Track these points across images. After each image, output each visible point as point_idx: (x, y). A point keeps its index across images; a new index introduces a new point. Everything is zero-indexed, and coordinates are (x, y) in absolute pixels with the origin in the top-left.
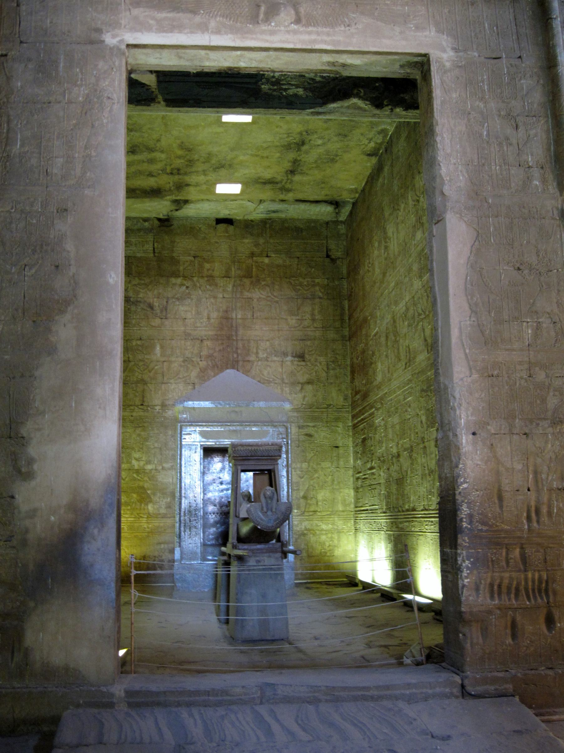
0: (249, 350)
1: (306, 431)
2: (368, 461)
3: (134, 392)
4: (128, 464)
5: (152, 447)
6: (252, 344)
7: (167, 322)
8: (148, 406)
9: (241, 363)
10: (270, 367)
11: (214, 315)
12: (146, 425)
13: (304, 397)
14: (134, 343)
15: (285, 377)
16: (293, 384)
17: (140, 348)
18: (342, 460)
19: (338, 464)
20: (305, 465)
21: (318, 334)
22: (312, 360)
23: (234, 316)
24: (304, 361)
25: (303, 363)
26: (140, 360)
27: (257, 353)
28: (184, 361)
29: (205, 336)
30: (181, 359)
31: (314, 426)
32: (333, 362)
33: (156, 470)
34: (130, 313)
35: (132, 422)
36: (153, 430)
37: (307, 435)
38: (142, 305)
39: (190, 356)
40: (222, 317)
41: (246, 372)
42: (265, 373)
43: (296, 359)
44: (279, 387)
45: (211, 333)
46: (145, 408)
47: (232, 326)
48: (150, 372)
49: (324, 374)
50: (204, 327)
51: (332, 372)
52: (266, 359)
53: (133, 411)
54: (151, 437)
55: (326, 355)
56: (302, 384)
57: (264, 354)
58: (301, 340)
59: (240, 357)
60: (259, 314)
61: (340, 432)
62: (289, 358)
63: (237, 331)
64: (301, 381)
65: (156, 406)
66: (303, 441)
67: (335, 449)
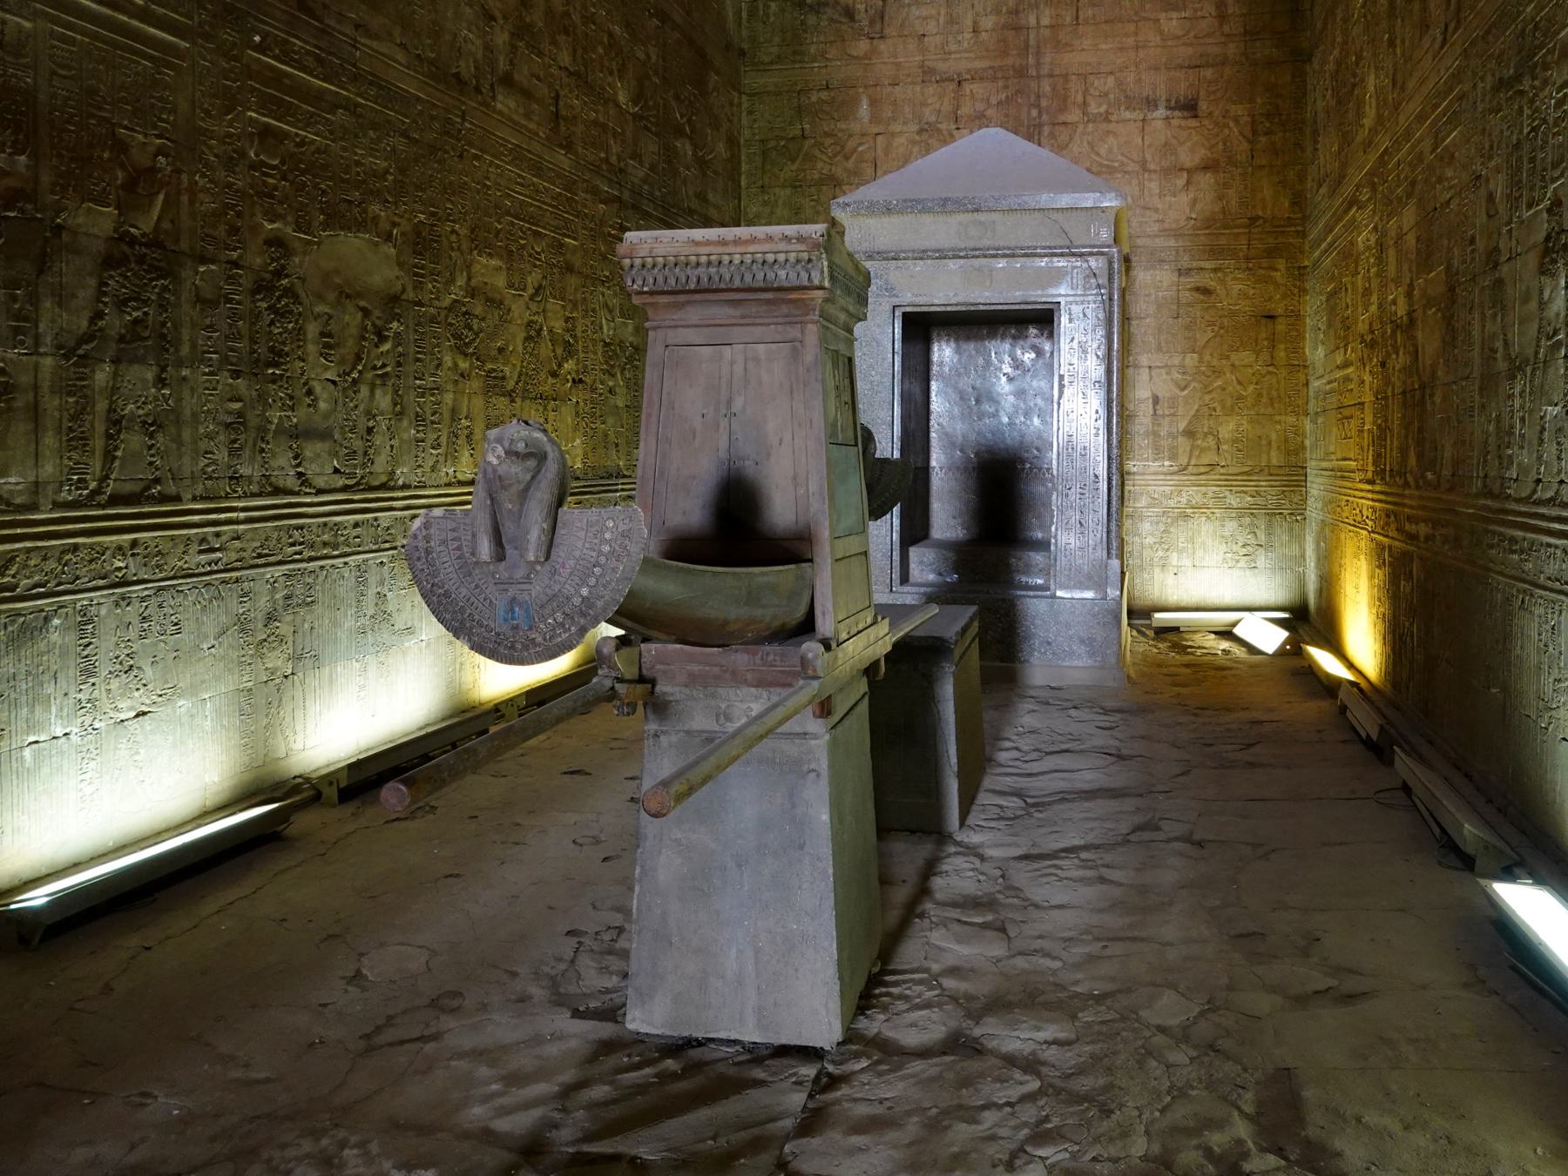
0: (1065, 98)
1: (1195, 280)
6: (1075, 86)
7: (883, 46)
9: (1046, 130)
10: (1115, 134)
11: (988, 22)
13: (1195, 201)
14: (814, 99)
15: (1148, 157)
16: (1166, 172)
17: (826, 108)
18: (1282, 346)
20: (1191, 360)
21: (1232, 50)
22: (1216, 113)
23: (1032, 20)
24: (1196, 117)
25: (1193, 123)
26: (826, 134)
27: (1085, 103)
28: (920, 132)
29: (969, 71)
30: (916, 128)
31: (1215, 270)
32: (1268, 116)
34: (805, 31)
37: (1197, 289)
38: (829, 10)
39: (933, 119)
40: (1005, 27)
41: (1060, 149)
42: (1103, 151)
43: (1177, 113)
44: (1135, 182)
45: (979, 64)
47: (1027, 46)
48: (847, 158)
49: (1245, 146)
50: (967, 51)
51: (1263, 139)
52: (1106, 118)
55: (1252, 100)
56: (1189, 171)
57: (1100, 105)
58: (1190, 67)
59: (1045, 117)
60: (1090, 12)
61: (1279, 280)
62: (1161, 112)
63: (1038, 53)
64: (1188, 164)
66: (1189, 305)
67: (1264, 321)
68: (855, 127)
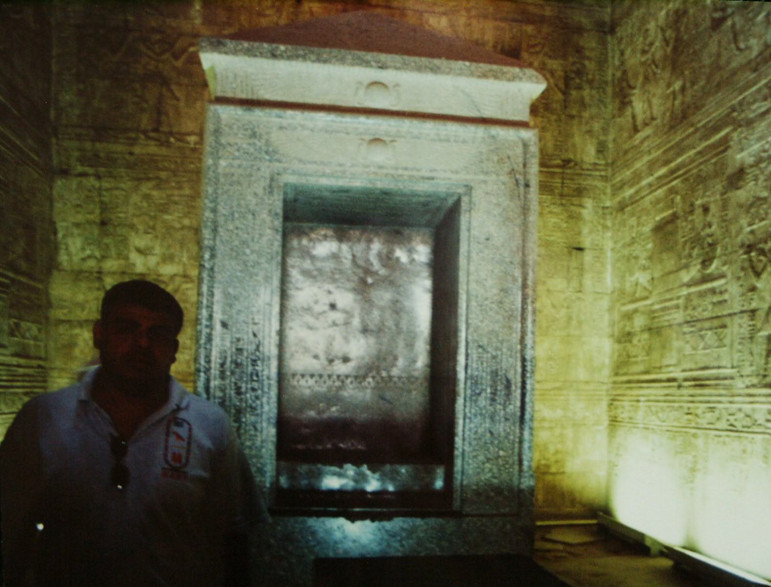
2: (686, 267)
3: (136, 99)
4: (122, 262)
5: (178, 226)
8: (171, 134)
12: (163, 175)
19: (581, 284)
33: (185, 276)
35: (130, 166)
36: (180, 188)
46: (163, 139)
48: (176, 57)
53: (133, 142)
54: (176, 203)
65: (189, 134)
67: (574, 252)
68: (186, 27)
